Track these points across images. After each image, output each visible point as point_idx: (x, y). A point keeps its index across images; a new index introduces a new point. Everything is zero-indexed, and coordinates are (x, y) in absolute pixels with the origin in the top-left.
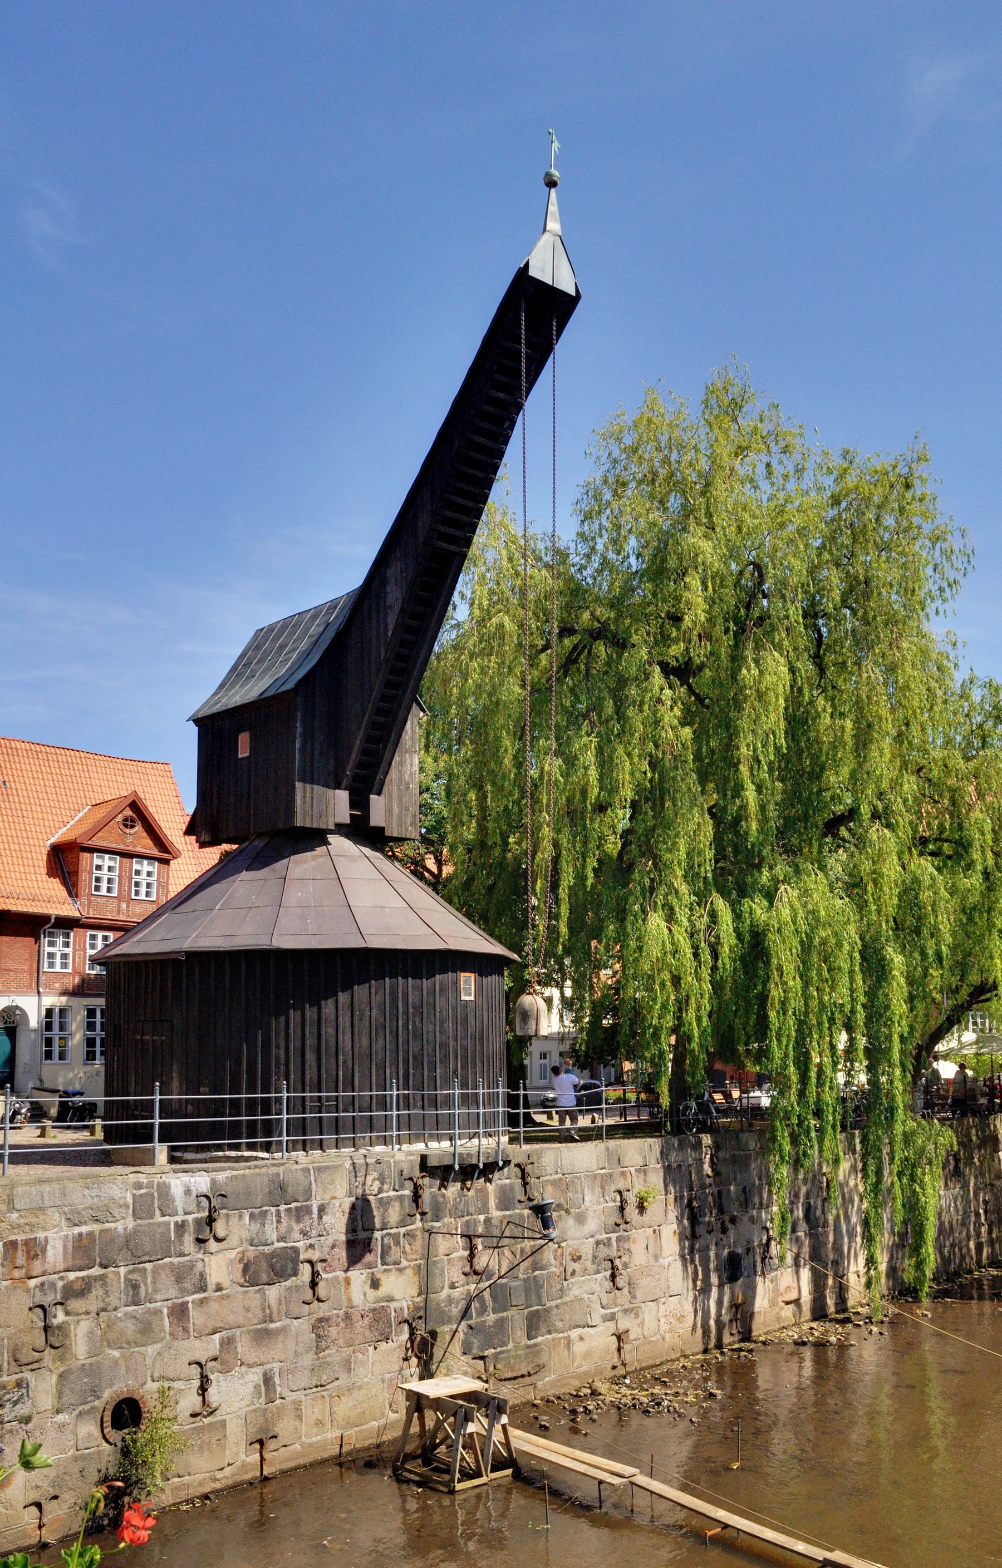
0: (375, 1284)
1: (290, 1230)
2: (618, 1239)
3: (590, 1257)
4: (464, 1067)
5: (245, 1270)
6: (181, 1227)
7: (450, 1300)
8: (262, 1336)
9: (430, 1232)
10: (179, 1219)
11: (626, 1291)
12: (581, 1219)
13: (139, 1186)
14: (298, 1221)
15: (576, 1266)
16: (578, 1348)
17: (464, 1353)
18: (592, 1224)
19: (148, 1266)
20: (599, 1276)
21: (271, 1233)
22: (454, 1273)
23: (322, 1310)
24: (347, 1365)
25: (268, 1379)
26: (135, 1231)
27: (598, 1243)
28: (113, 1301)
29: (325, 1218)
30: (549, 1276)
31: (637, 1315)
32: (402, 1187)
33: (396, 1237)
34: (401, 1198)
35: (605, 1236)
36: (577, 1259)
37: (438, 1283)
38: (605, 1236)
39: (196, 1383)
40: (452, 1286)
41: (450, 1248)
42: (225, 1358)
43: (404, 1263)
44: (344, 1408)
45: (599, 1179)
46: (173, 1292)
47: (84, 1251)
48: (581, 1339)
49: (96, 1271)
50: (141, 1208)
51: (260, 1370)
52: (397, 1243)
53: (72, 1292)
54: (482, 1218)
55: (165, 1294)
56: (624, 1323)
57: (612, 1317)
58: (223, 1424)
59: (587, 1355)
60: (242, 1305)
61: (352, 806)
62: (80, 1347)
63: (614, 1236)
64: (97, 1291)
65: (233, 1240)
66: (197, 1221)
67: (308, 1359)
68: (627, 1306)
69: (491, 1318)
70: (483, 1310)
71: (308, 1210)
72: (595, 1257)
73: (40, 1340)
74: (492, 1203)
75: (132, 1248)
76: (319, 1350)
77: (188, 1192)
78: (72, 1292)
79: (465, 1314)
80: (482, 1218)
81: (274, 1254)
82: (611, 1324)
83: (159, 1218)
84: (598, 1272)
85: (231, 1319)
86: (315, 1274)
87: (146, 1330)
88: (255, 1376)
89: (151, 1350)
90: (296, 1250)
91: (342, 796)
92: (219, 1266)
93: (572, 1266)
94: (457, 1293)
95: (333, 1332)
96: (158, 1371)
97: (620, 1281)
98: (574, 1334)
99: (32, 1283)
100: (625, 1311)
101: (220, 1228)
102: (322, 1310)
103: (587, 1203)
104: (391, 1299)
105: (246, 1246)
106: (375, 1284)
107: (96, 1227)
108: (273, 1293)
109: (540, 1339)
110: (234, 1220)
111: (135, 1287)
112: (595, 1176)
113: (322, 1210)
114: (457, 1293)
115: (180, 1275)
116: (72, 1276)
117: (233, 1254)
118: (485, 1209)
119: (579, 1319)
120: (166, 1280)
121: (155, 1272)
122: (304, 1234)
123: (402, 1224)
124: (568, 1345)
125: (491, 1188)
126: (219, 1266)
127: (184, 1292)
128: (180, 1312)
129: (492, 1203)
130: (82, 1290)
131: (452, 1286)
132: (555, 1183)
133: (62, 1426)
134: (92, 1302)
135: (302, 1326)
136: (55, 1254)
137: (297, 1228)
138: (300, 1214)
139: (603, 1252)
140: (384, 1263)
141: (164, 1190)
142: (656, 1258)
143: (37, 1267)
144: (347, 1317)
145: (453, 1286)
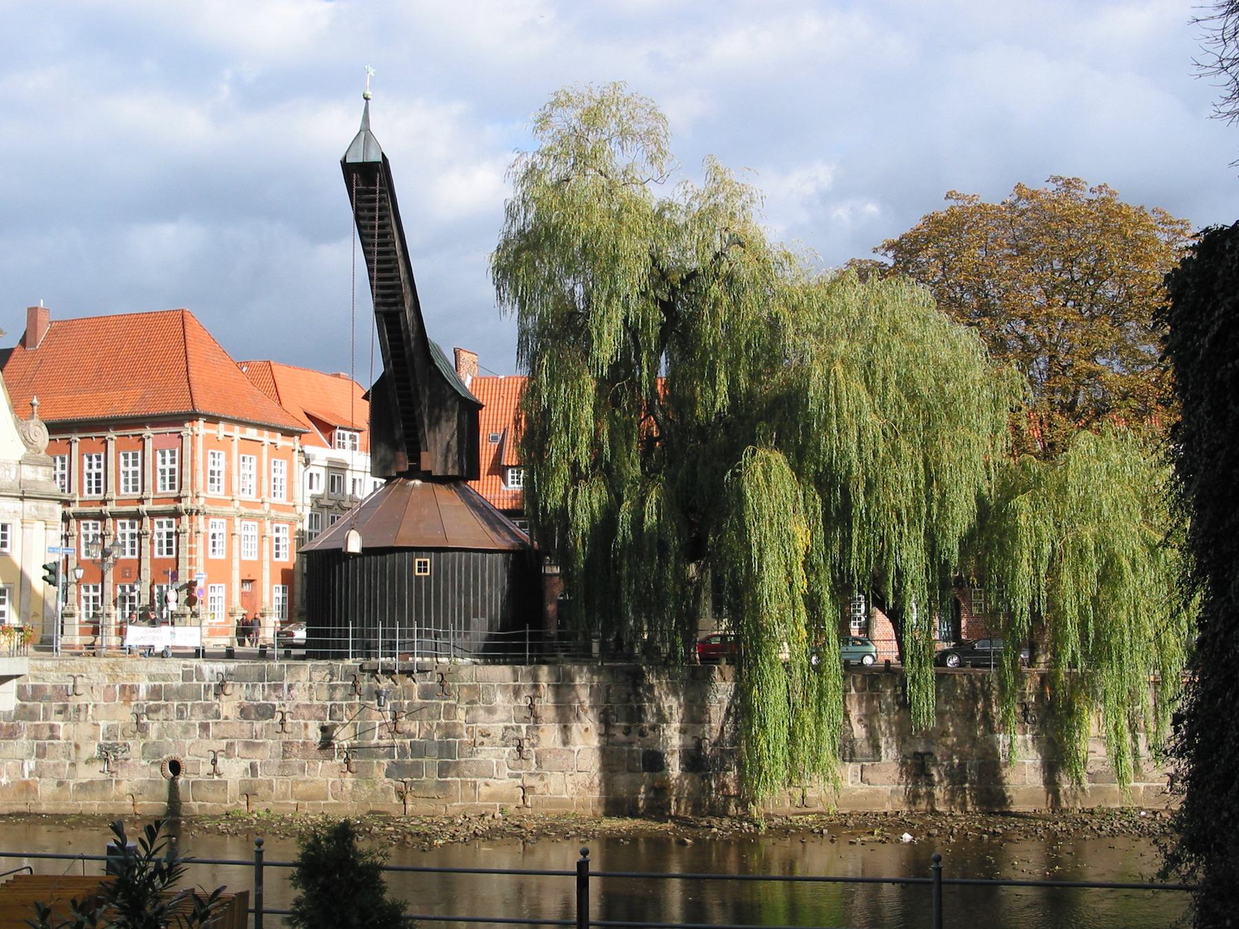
1: (270, 695)
2: (527, 728)
3: (500, 736)
5: (241, 712)
6: (207, 688)
10: (207, 683)
12: (491, 711)
13: (185, 666)
14: (275, 691)
15: (485, 740)
16: (483, 790)
17: (387, 776)
19: (189, 703)
20: (507, 750)
23: (285, 737)
25: (253, 766)
27: (506, 728)
31: (542, 779)
34: (345, 686)
35: (514, 724)
38: (514, 724)
40: (380, 738)
41: (379, 718)
42: (229, 752)
46: (201, 716)
47: (155, 693)
48: (487, 785)
49: (163, 702)
50: (187, 676)
51: (248, 762)
54: (406, 702)
56: (530, 782)
57: (518, 776)
58: (226, 783)
59: (492, 797)
62: (153, 734)
63: (524, 726)
64: (163, 711)
67: (278, 761)
68: (533, 770)
71: (282, 686)
74: (416, 694)
75: (180, 694)
78: (149, 710)
80: (406, 702)
81: (259, 706)
82: (519, 782)
83: (195, 681)
84: (506, 746)
85: (232, 734)
86: (283, 719)
88: (246, 764)
89: (188, 742)
90: (274, 706)
92: (227, 707)
93: (480, 739)
95: (295, 750)
96: (194, 751)
98: (480, 781)
99: (133, 704)
100: (531, 774)
101: (228, 691)
102: (285, 737)
105: (243, 700)
107: (163, 684)
108: (258, 725)
110: (237, 687)
111: (182, 712)
113: (290, 687)
114: (384, 742)
115: (206, 709)
116: (151, 703)
117: (236, 703)
118: (410, 697)
120: (197, 711)
121: (193, 706)
122: (279, 698)
123: (345, 699)
124: (475, 786)
125: (416, 686)
126: (227, 707)
127: (207, 717)
128: (205, 727)
129: (416, 694)
130: (157, 710)
132: (473, 689)
133: (143, 767)
134: (161, 715)
135: (273, 744)
138: (276, 688)
141: (199, 671)
144: (304, 744)
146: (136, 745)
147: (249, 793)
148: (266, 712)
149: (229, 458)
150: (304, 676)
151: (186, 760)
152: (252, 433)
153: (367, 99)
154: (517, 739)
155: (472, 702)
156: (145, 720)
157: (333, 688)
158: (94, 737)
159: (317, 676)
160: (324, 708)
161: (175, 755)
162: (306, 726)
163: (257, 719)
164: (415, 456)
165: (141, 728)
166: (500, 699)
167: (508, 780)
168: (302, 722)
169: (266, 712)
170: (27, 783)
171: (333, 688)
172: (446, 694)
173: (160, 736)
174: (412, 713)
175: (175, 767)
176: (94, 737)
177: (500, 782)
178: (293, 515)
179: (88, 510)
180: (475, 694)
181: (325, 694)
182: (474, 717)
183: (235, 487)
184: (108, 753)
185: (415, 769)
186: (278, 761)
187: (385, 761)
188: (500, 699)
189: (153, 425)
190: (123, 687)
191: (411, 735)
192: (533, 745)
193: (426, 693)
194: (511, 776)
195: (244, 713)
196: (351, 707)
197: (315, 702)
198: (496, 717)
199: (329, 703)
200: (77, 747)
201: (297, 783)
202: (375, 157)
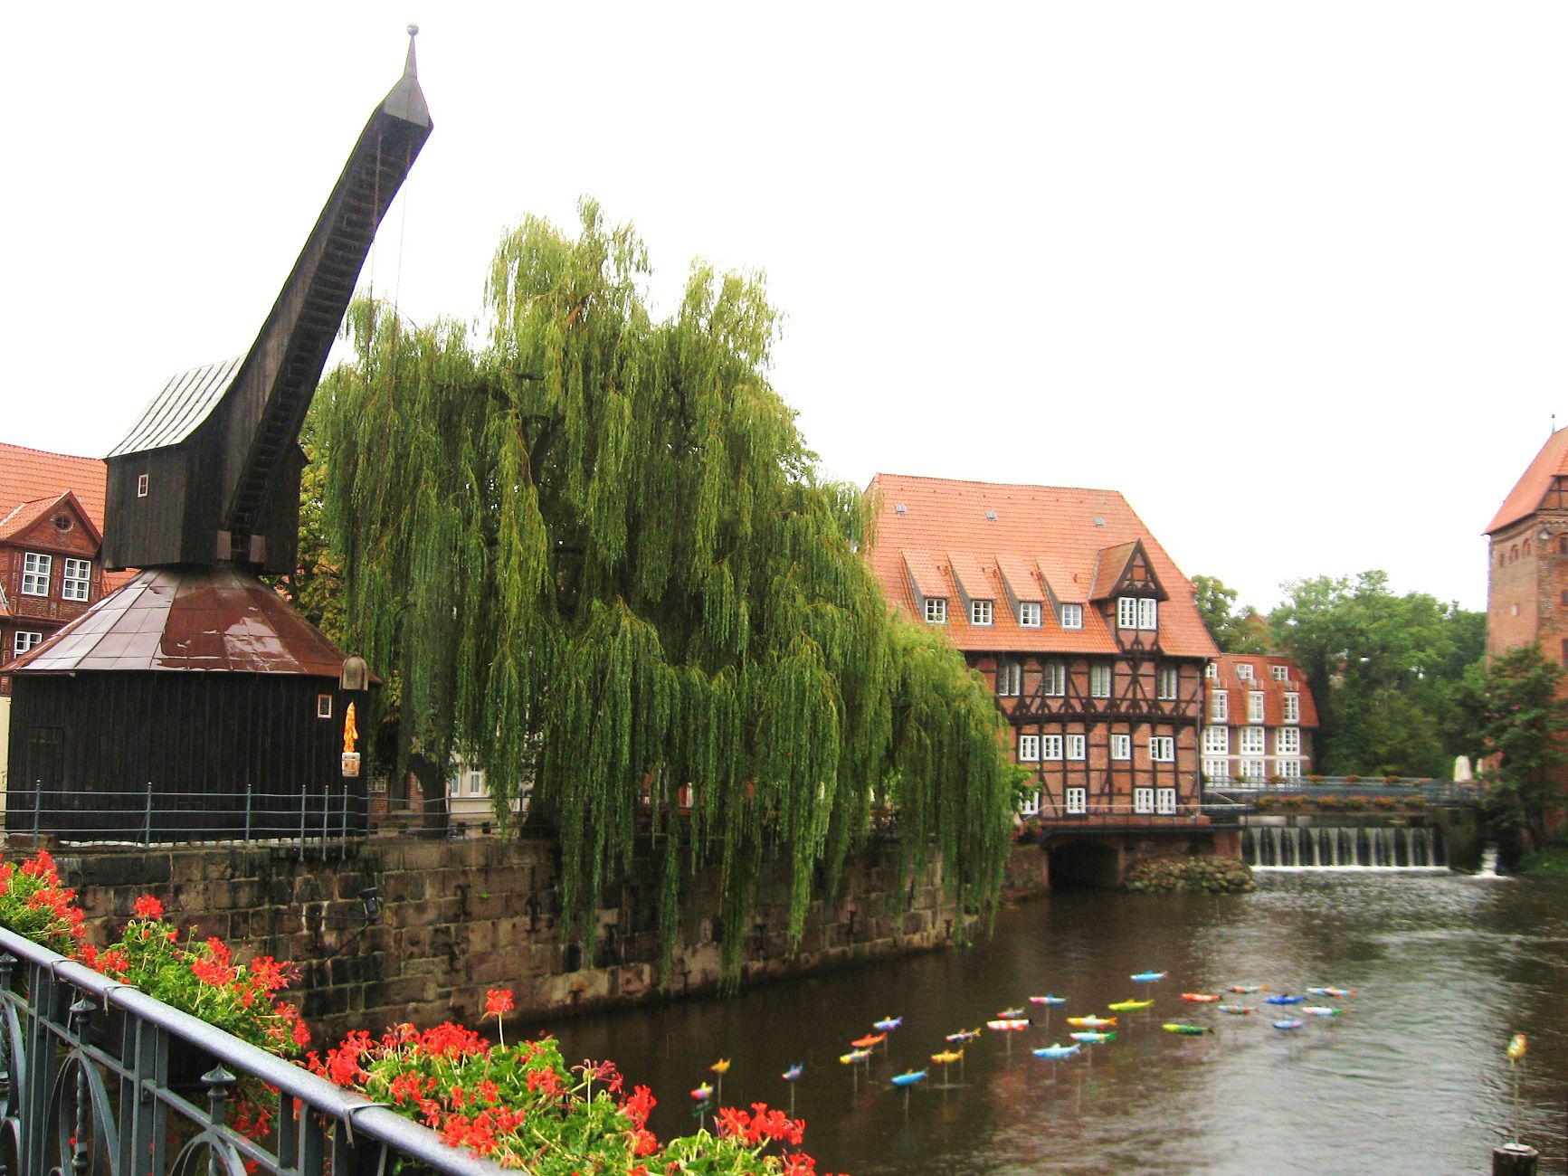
2: (457, 930)
9: (277, 912)
11: (463, 974)
12: (421, 909)
15: (415, 949)
18: (431, 914)
27: (436, 931)
29: (182, 897)
31: (472, 995)
32: (253, 875)
33: (245, 917)
36: (415, 943)
43: (251, 937)
52: (245, 921)
54: (326, 903)
61: (234, 543)
63: (453, 926)
65: (100, 910)
70: (323, 982)
72: (433, 943)
91: (225, 537)
97: (460, 964)
103: (428, 896)
109: (377, 1009)
110: (100, 895)
117: (98, 922)
125: (336, 878)
139: (441, 938)
140: (233, 936)
150: (197, 875)
155: (400, 898)
157: (235, 888)
159: (214, 872)
160: (222, 920)
167: (438, 1003)
171: (235, 888)
177: (428, 1006)
188: (429, 892)
192: (464, 952)
199: (228, 913)
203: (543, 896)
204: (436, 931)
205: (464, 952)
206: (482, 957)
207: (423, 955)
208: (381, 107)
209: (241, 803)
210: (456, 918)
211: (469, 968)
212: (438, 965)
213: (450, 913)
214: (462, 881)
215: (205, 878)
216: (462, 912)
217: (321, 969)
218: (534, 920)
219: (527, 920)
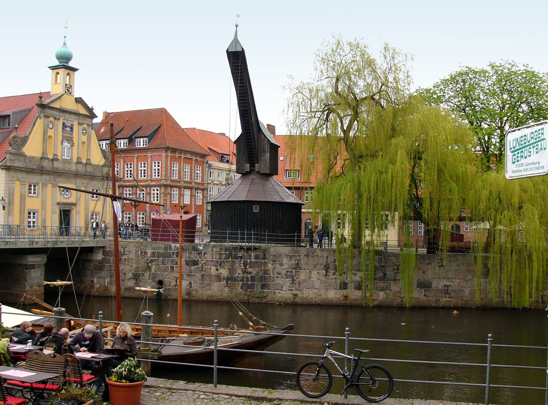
0: (217, 270)
4: (254, 227)
5: (186, 263)
6: (173, 253)
7: (238, 277)
8: (189, 275)
11: (297, 284)
15: (279, 276)
18: (285, 266)
21: (192, 256)
22: (239, 271)
24: (209, 285)
25: (190, 283)
26: (164, 252)
27: (287, 271)
28: (159, 263)
30: (270, 277)
33: (224, 262)
34: (226, 254)
37: (234, 272)
39: (175, 281)
40: (239, 274)
44: (209, 292)
45: (289, 257)
50: (166, 248)
52: (224, 263)
53: (152, 261)
55: (169, 265)
56: (296, 292)
57: (292, 290)
59: (281, 297)
60: (185, 268)
62: (153, 270)
63: (294, 271)
64: (157, 262)
66: (177, 253)
67: (200, 281)
69: (250, 283)
70: (248, 280)
71: (201, 253)
73: (146, 268)
75: (164, 255)
76: (202, 280)
77: (175, 247)
78: (152, 261)
79: (242, 280)
82: (291, 292)
87: (166, 270)
88: (188, 282)
90: (198, 261)
91: (248, 165)
94: (240, 275)
95: (206, 278)
98: (277, 291)
102: (203, 273)
104: (221, 274)
106: (217, 270)
108: (192, 268)
112: (288, 255)
114: (240, 275)
115: (172, 261)
118: (250, 259)
119: (278, 288)
120: (170, 262)
124: (275, 293)
128: (172, 268)
131: (239, 274)
135: (199, 275)
136: (149, 254)
137: (198, 256)
139: (289, 274)
142: (310, 278)
143: (146, 256)
145: (239, 273)
146: (147, 275)
147: (189, 294)
148: (195, 263)
149: (180, 165)
150: (210, 250)
151: (166, 281)
152: (189, 156)
153: (237, 26)
154: (291, 276)
156: (150, 265)
158: (130, 271)
159: (215, 250)
160: (217, 262)
161: (160, 278)
162: (210, 268)
163: (192, 266)
164: (252, 166)
165: (149, 268)
166: (285, 261)
167: (288, 292)
168: (209, 267)
169: (195, 263)
170: (106, 287)
172: (264, 258)
173: (155, 271)
174: (252, 265)
175: (161, 283)
176: (130, 271)
178: (203, 187)
179: (127, 184)
180: (276, 259)
181: (218, 257)
182: (275, 267)
183: (182, 177)
184: (136, 277)
185: (252, 286)
186: (200, 281)
187: (240, 283)
188: (285, 261)
189: (152, 152)
190: (141, 252)
191: (250, 273)
192: (297, 278)
193: (257, 257)
194: (289, 290)
195: (187, 263)
196: (228, 262)
197: (214, 260)
198: (283, 267)
200: (125, 274)
201: (207, 290)
202: (239, 49)
203: (331, 266)
204: (287, 271)
205: (297, 278)
206: (304, 281)
207: (282, 278)
208: (227, 51)
209: (226, 234)
210: (295, 268)
211: (299, 283)
212: (288, 281)
213: (293, 267)
214: (298, 258)
215: (212, 251)
216: (297, 266)
217: (247, 278)
218: (327, 272)
219: (324, 272)
